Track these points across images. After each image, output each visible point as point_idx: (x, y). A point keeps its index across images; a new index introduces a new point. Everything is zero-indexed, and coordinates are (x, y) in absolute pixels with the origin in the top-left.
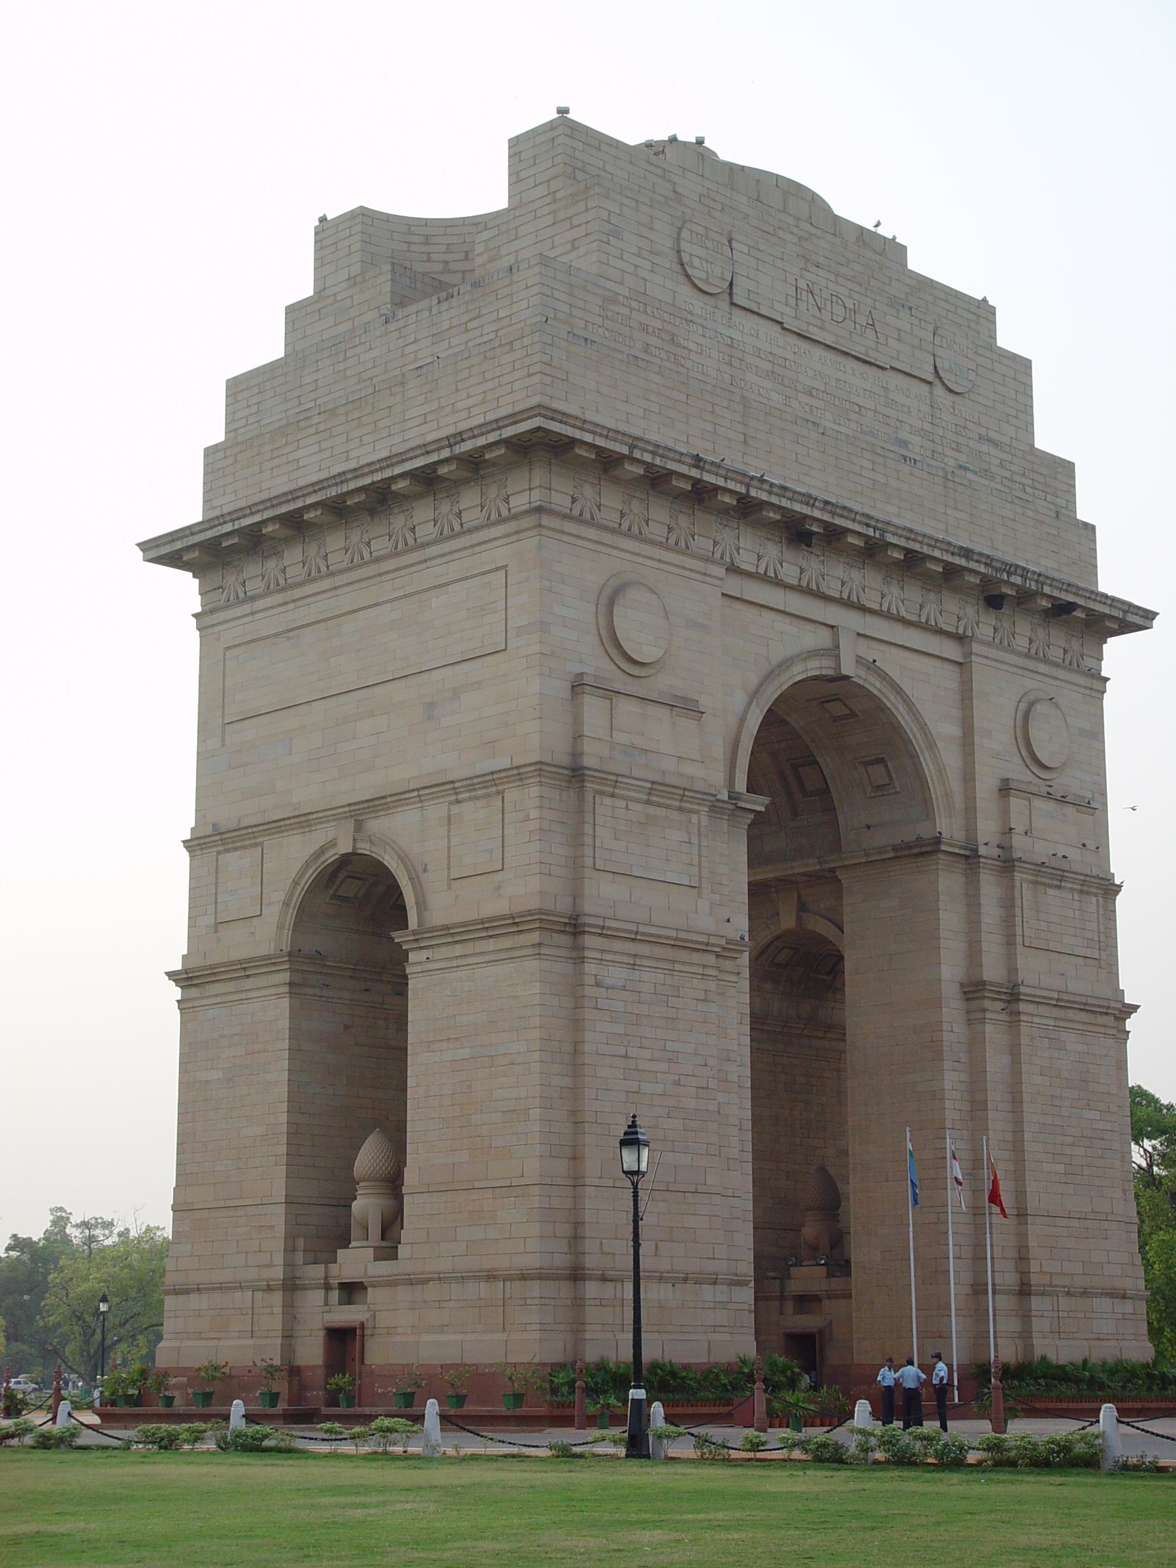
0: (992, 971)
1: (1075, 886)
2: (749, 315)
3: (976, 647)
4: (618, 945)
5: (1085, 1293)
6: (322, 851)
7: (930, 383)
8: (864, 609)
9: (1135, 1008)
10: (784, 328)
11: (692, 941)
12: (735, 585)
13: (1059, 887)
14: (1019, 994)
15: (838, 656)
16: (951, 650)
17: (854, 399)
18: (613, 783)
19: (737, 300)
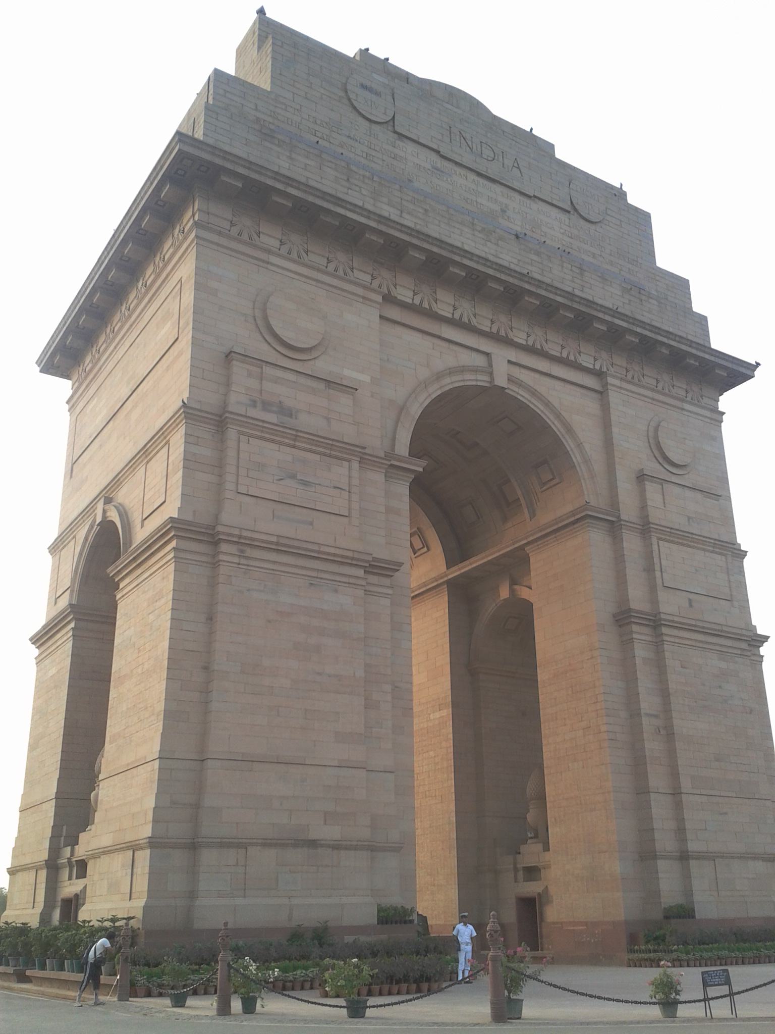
3: (610, 380)
6: (92, 527)
12: (394, 313)
14: (660, 619)
15: (491, 374)
16: (591, 381)
19: (398, 129)
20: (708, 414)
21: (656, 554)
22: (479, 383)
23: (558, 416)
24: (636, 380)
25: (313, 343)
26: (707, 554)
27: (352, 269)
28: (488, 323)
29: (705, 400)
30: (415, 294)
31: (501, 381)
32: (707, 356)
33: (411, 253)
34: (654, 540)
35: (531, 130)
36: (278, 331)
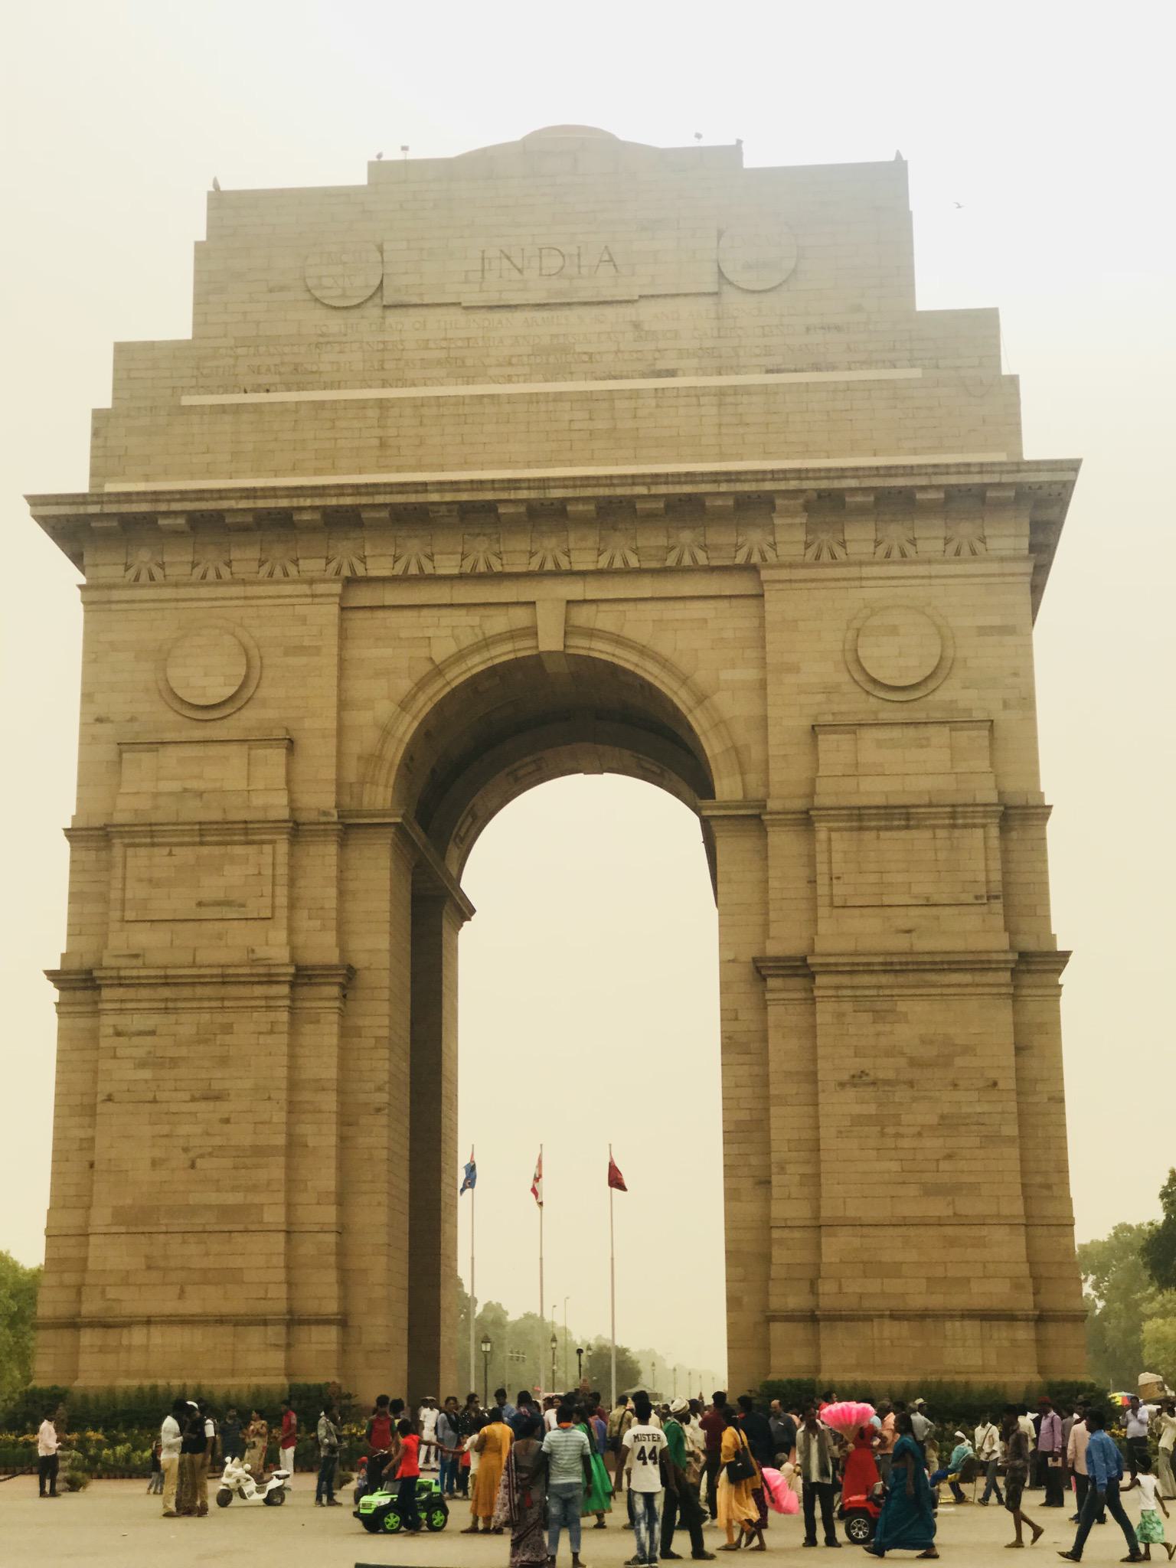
0: (786, 942)
1: (940, 822)
2: (412, 311)
3: (765, 574)
4: (144, 993)
5: (923, 1315)
7: (716, 294)
8: (583, 574)
9: (1066, 955)
10: (466, 308)
11: (181, 976)
13: (907, 827)
16: (741, 585)
17: (578, 349)
18: (148, 833)
20: (994, 568)
21: (821, 858)
22: (520, 654)
23: (665, 663)
24: (826, 556)
25: (230, 691)
26: (942, 833)
27: (296, 562)
28: (524, 559)
29: (992, 544)
30: (396, 559)
31: (550, 640)
32: (953, 480)
33: (365, 515)
34: (822, 835)
35: (698, 136)
36: (180, 693)
